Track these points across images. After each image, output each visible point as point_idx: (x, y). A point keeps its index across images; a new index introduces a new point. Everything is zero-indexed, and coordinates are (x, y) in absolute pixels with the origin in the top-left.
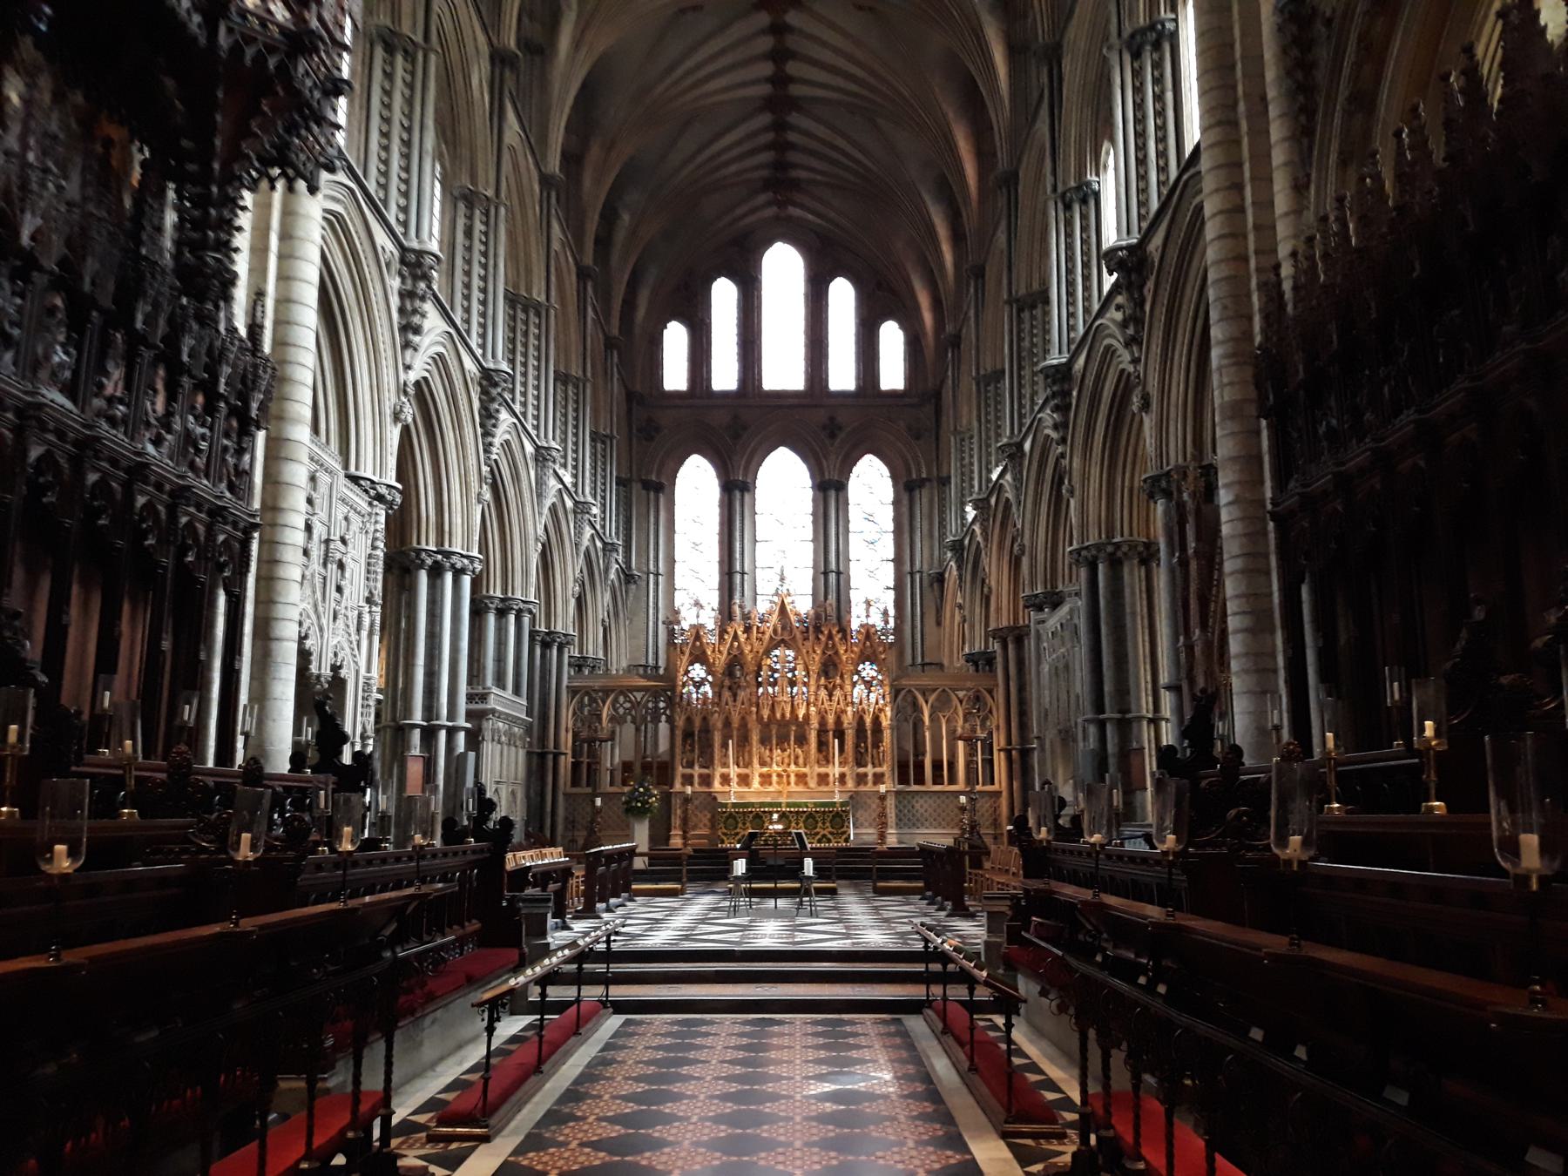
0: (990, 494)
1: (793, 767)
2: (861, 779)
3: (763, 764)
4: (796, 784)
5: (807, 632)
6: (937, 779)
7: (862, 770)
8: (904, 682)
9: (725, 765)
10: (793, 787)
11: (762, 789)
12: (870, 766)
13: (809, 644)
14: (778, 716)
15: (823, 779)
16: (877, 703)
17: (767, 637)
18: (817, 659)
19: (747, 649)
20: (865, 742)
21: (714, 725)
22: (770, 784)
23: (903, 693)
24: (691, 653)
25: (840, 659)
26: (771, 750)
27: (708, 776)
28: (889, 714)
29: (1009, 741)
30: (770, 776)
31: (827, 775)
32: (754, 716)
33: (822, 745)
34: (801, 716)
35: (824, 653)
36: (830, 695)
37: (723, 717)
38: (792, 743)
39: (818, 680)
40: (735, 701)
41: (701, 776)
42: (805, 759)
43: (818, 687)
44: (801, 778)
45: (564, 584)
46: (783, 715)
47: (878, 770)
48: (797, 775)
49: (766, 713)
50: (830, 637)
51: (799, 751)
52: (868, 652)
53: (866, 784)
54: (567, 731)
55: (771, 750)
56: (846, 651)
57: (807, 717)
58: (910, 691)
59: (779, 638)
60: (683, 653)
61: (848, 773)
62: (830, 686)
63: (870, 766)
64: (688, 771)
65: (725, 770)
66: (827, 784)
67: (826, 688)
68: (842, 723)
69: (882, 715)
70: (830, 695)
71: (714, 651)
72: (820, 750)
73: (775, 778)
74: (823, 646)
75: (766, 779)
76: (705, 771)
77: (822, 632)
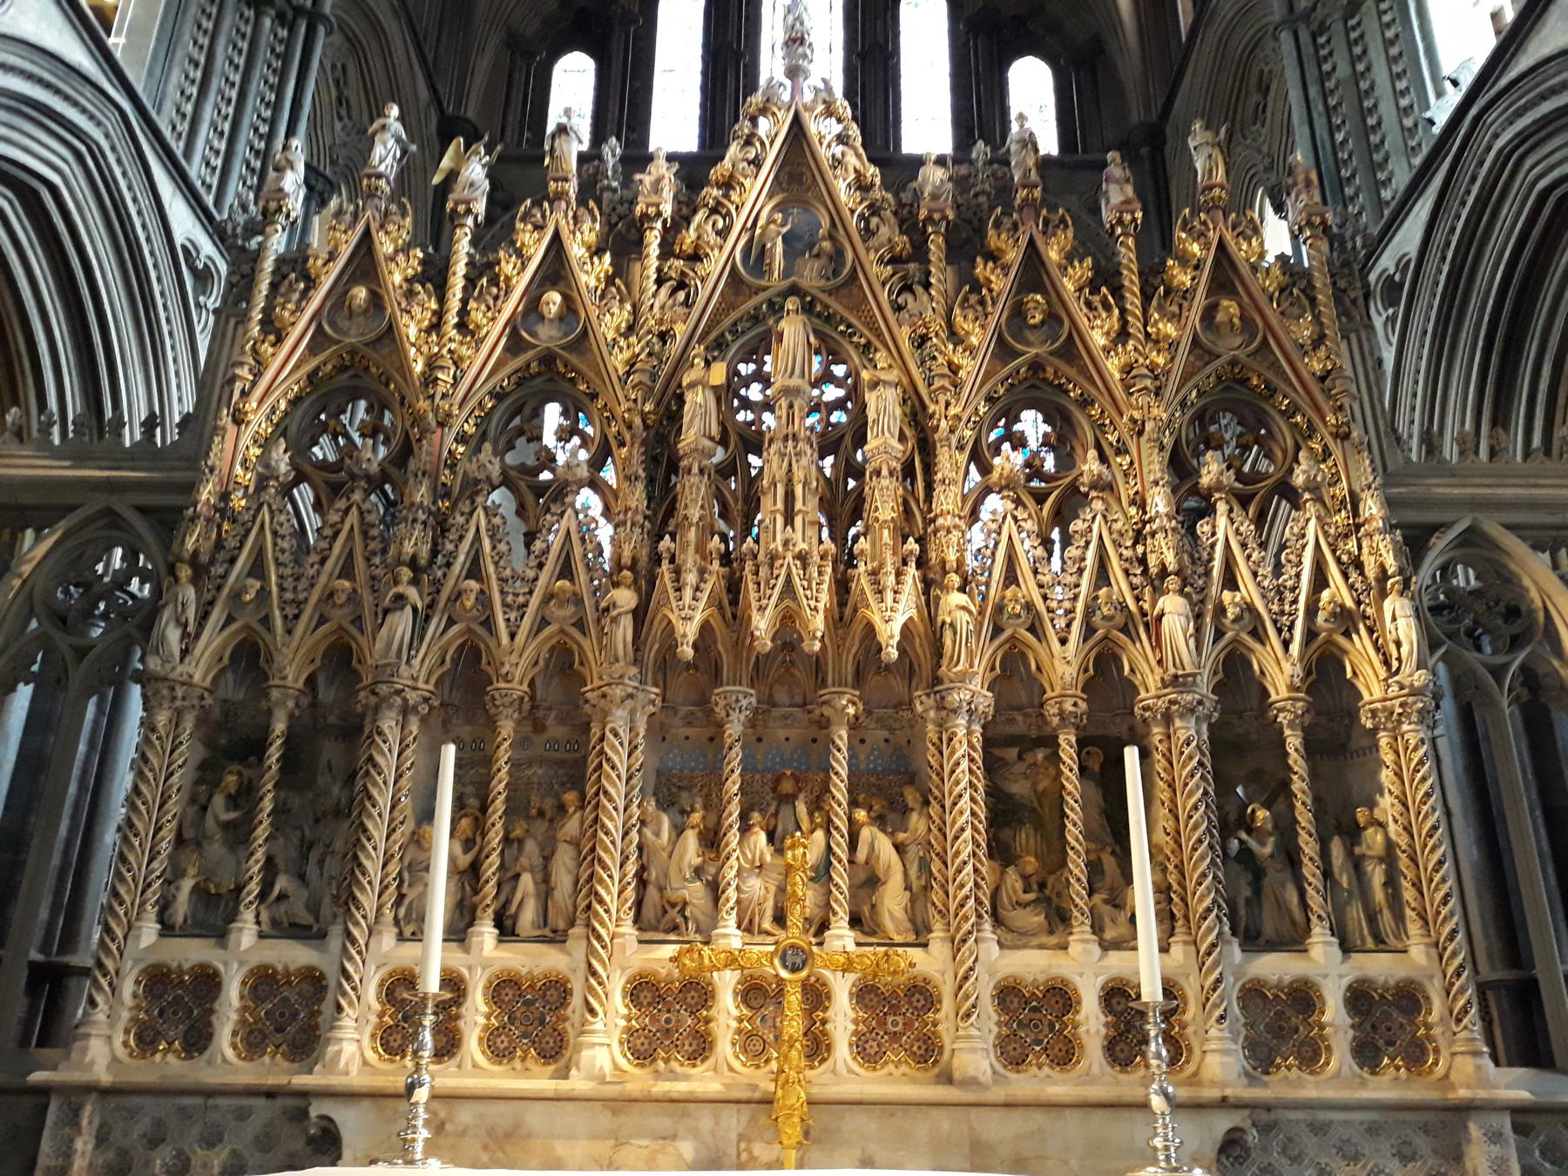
1: (842, 936)
4: (867, 1052)
5: (920, 252)
7: (1274, 967)
8: (1442, 489)
11: (639, 1080)
12: (1322, 944)
13: (928, 307)
14: (762, 624)
17: (714, 265)
18: (969, 367)
19: (610, 322)
20: (1277, 794)
21: (386, 672)
22: (701, 1048)
23: (1439, 545)
24: (319, 341)
26: (712, 840)
27: (314, 982)
30: (698, 993)
31: (1061, 997)
32: (624, 630)
34: (890, 632)
35: (1003, 351)
38: (840, 791)
41: (263, 982)
42: (918, 896)
48: (864, 994)
50: (1033, 274)
51: (879, 844)
52: (1231, 346)
53: (1311, 1055)
55: (712, 840)
56: (1123, 335)
58: (1472, 539)
59: (776, 278)
60: (273, 328)
61: (1191, 988)
63: (1322, 944)
64: (191, 952)
66: (1065, 1054)
68: (1130, 689)
69: (1360, 653)
71: (436, 326)
72: (1000, 852)
73: (727, 1010)
74: (998, 314)
76: (293, 955)
77: (993, 257)
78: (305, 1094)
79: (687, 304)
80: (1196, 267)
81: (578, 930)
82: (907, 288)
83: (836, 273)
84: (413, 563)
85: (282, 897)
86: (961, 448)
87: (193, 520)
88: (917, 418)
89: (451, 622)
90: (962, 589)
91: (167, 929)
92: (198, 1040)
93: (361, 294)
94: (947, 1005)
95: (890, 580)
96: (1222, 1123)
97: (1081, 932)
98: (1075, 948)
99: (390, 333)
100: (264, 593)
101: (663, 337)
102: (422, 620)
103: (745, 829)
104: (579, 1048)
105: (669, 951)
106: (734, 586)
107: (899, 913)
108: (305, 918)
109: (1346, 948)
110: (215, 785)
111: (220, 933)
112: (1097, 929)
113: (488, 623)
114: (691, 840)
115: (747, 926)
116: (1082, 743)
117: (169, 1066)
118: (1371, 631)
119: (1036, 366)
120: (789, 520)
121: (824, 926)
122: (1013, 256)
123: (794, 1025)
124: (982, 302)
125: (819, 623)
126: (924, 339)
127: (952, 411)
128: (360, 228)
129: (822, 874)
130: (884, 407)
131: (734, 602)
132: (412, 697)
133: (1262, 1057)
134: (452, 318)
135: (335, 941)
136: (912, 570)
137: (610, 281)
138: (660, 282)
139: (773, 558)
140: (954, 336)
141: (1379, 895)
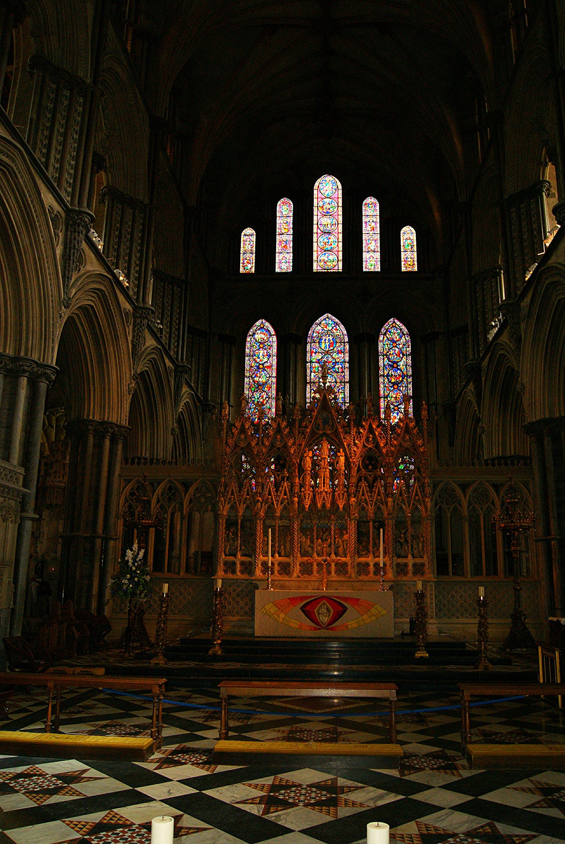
0: (523, 296)
1: (333, 556)
2: (401, 569)
3: (304, 554)
6: (477, 571)
7: (401, 561)
9: (266, 554)
10: (334, 576)
12: (410, 556)
15: (363, 568)
16: (417, 495)
18: (359, 451)
21: (257, 514)
25: (380, 451)
28: (429, 505)
29: (548, 532)
31: (367, 564)
33: (361, 536)
34: (341, 506)
36: (371, 487)
37: (265, 507)
39: (359, 470)
40: (277, 491)
41: (242, 563)
43: (360, 480)
44: (342, 568)
45: (120, 379)
46: (324, 505)
47: (418, 561)
49: (307, 503)
50: (371, 430)
52: (407, 445)
53: (406, 574)
54: (117, 517)
56: (386, 444)
57: (347, 506)
62: (371, 479)
63: (410, 556)
65: (266, 558)
67: (366, 479)
70: (371, 487)
71: (257, 444)
74: (363, 439)
75: (306, 569)
77: (363, 427)
78: (252, 580)
79: (305, 438)
80: (402, 429)
81: (291, 555)
82: (346, 433)
83: (333, 429)
84: (260, 493)
85: (243, 549)
86: (356, 466)
87: (221, 485)
88: (347, 459)
89: (266, 503)
90: (354, 497)
91: (226, 555)
92: (234, 572)
93: (243, 436)
94: (349, 566)
95: (341, 497)
96: (390, 584)
97: (371, 555)
98: (370, 558)
99: (249, 445)
100: (234, 499)
101: (300, 445)
102: (262, 503)
103: (317, 539)
104: (293, 573)
105: (306, 558)
106: (314, 496)
107: (342, 552)
108: (247, 553)
109: (414, 557)
110: (230, 531)
111: (235, 556)
112: (374, 554)
113: (273, 503)
114: (308, 540)
115: (318, 555)
116: (374, 523)
117: (230, 576)
118: (424, 504)
119: (370, 449)
120: (324, 486)
121: (330, 554)
122: (367, 427)
123: (325, 570)
124: (360, 437)
125: (329, 505)
126: (349, 445)
127: (354, 460)
128: (241, 422)
129: (330, 546)
130: (342, 459)
131: (315, 499)
132: (262, 517)
133: (398, 573)
134: (260, 442)
135: (254, 558)
136: (346, 494)
137: (289, 433)
138: (299, 433)
139: (321, 492)
140: (355, 444)
141: (421, 549)
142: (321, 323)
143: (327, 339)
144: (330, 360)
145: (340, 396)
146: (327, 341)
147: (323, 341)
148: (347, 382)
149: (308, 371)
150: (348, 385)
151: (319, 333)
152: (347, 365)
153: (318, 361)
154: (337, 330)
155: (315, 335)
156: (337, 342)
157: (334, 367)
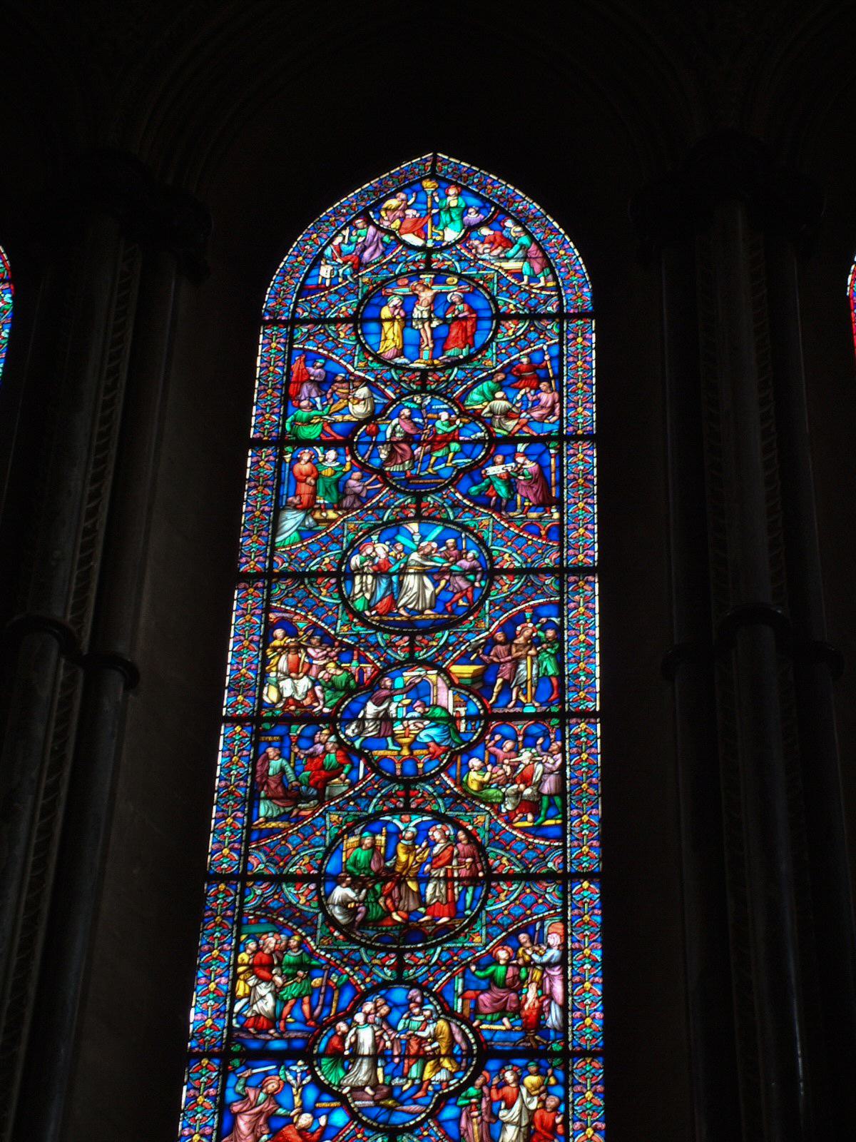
142: (377, 207)
143: (426, 296)
144: (441, 427)
145: (526, 671)
146: (420, 311)
147: (386, 312)
148: (583, 571)
149: (253, 501)
150: (594, 588)
151: (359, 265)
152: (584, 459)
153: (345, 439)
154: (509, 243)
155: (325, 271)
156: (500, 317)
157: (474, 471)
